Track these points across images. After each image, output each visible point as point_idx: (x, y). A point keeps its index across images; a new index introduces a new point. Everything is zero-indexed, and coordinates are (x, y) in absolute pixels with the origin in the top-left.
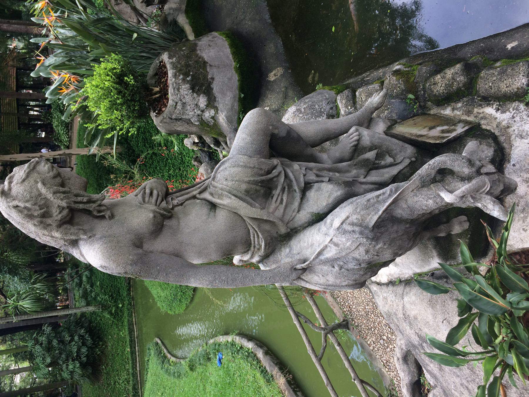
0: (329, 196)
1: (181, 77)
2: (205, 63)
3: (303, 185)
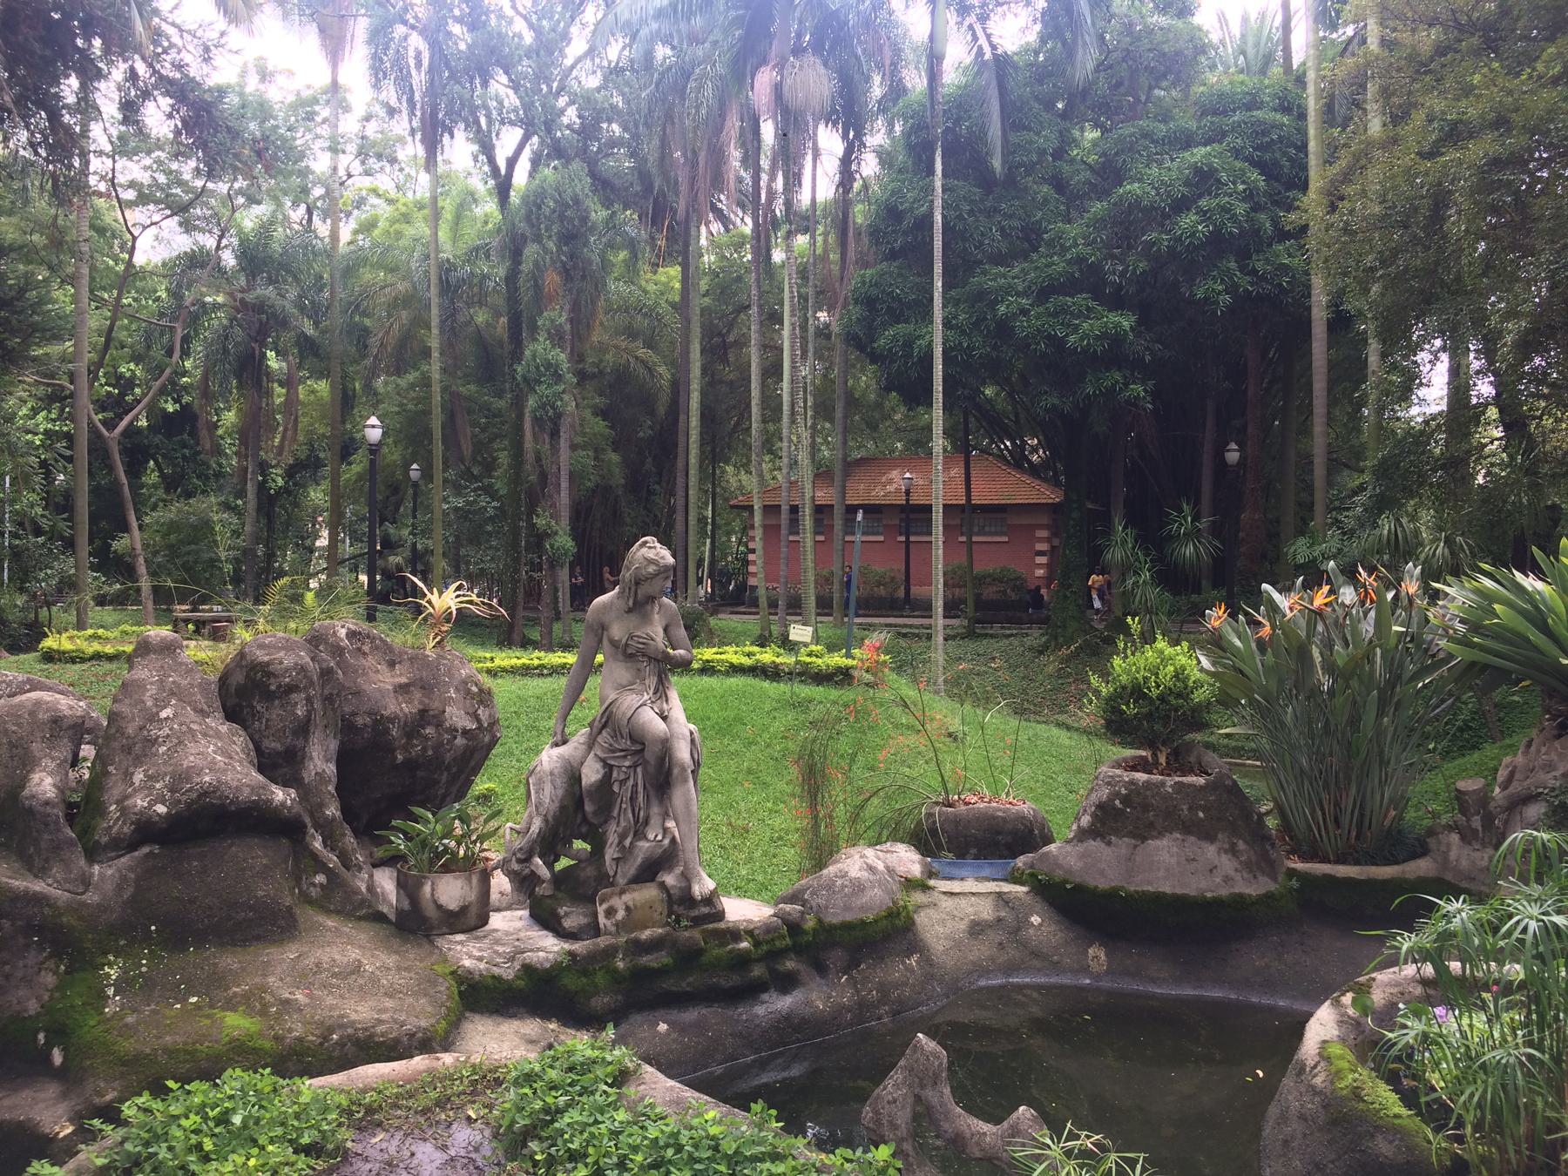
1: (1123, 791)
2: (1144, 839)
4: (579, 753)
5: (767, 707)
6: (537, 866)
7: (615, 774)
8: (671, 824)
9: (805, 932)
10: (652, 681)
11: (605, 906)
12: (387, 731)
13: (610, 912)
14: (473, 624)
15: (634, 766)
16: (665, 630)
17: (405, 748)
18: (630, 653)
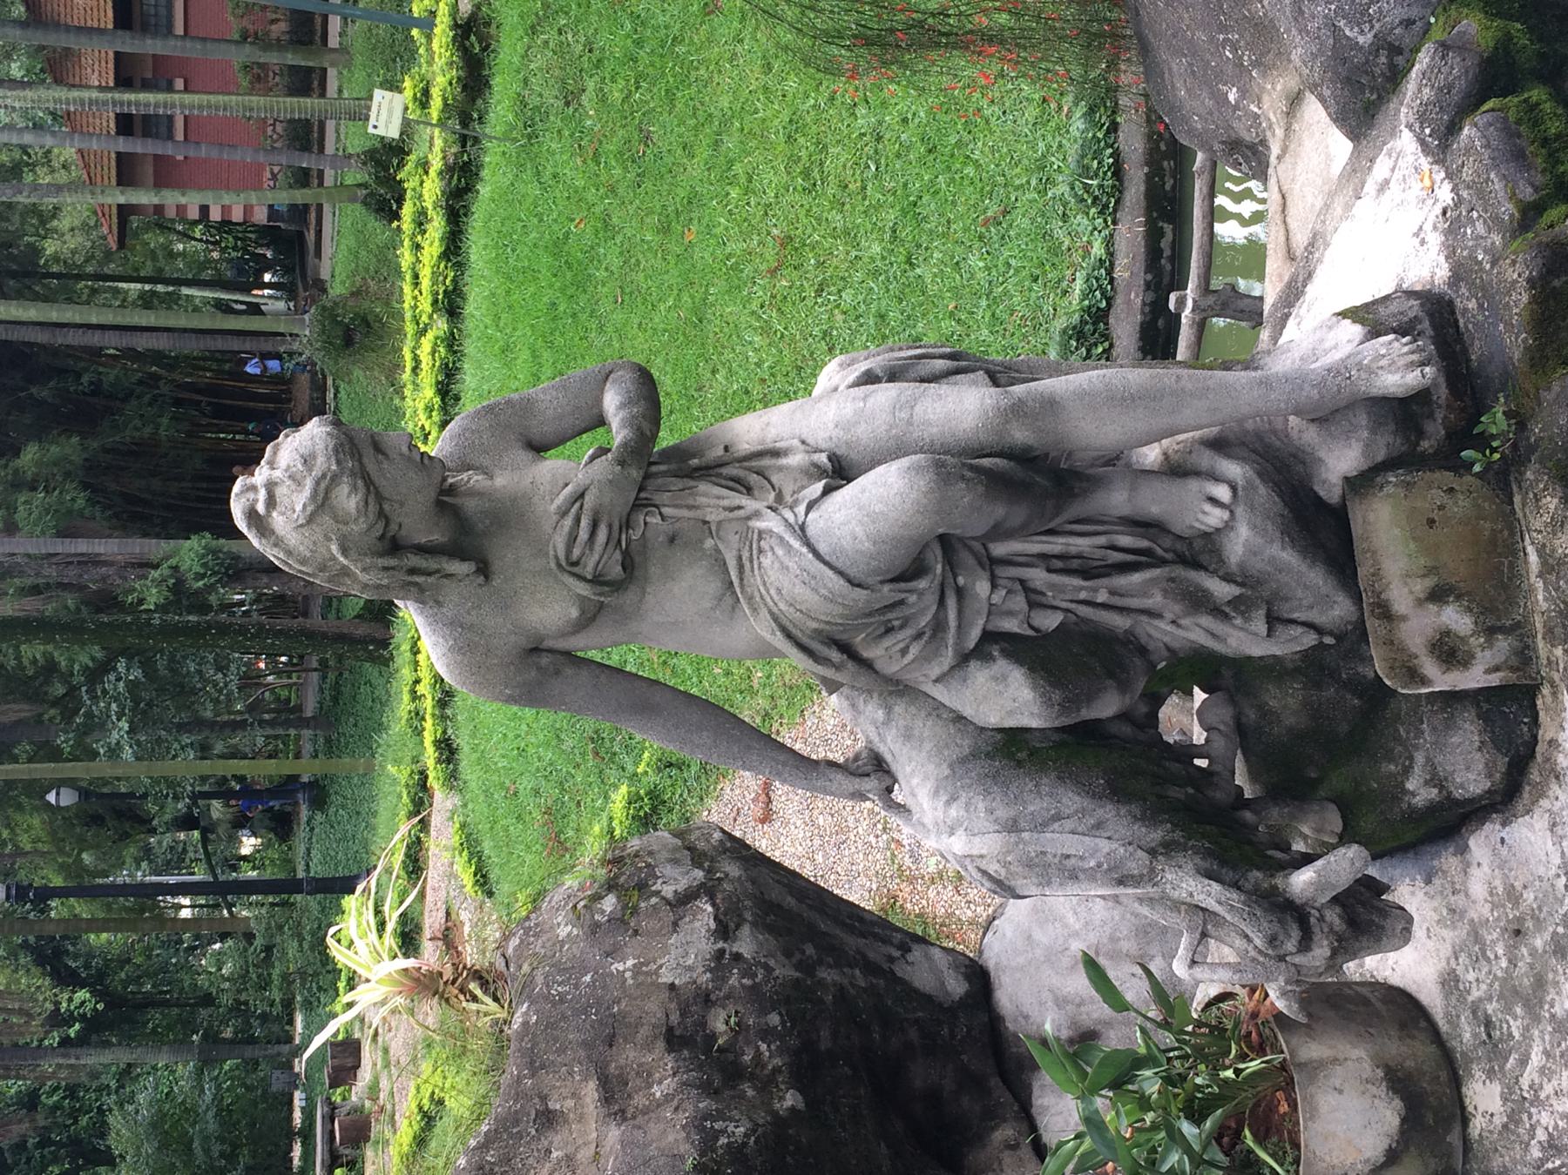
0: (1010, 713)
3: (972, 645)
4: (926, 728)
5: (534, 190)
6: (1319, 885)
7: (1011, 625)
8: (1151, 455)
9: (1505, 44)
10: (712, 499)
11: (1430, 668)
12: (737, 1152)
13: (1449, 651)
14: (335, 700)
15: (992, 565)
16: (538, 448)
17: (766, 1085)
18: (620, 569)
